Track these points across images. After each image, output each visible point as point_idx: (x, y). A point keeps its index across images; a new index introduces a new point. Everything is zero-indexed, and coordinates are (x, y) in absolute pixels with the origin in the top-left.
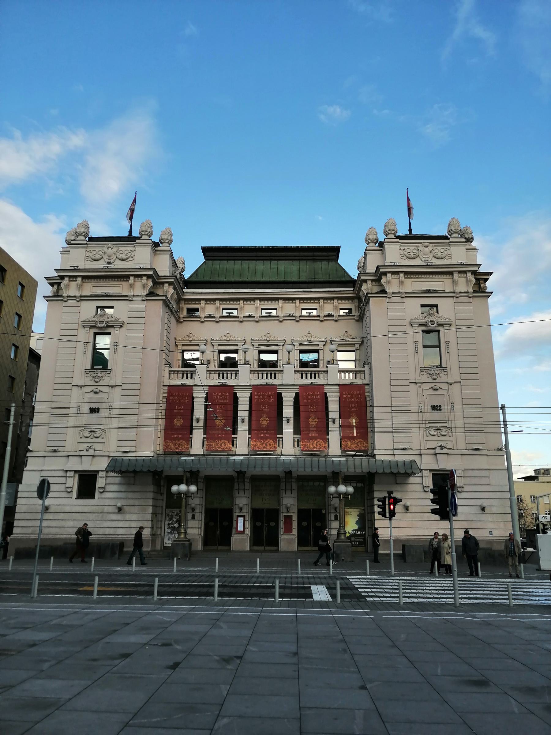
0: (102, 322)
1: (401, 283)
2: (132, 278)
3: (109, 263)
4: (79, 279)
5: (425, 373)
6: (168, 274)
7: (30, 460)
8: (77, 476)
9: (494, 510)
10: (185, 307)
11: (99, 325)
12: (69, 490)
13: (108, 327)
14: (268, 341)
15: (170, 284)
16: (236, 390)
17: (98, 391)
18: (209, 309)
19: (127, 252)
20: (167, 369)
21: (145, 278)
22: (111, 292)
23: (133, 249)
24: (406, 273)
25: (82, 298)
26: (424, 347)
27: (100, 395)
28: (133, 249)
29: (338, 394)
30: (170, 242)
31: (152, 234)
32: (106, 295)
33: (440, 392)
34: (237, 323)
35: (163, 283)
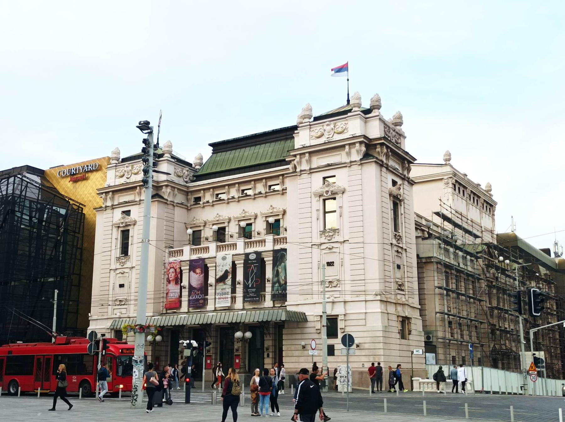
0: (122, 223)
1: (309, 161)
2: (347, 147)
3: (128, 178)
4: (111, 193)
5: (323, 236)
6: (379, 136)
7: (91, 322)
8: (113, 332)
9: (367, 346)
10: (192, 198)
11: (121, 225)
12: (318, 331)
13: (127, 226)
14: (244, 217)
15: (167, 186)
16: (207, 261)
17: (331, 247)
18: (208, 197)
19: (342, 125)
20: (167, 251)
21: (358, 145)
22: (332, 162)
23: (346, 122)
24: (310, 153)
25: (312, 171)
26: (335, 211)
27: (125, 274)
28: (346, 122)
29: (272, 258)
30: (379, 107)
31: (380, 99)
32: (126, 202)
33: (334, 250)
34: (225, 205)
35: (162, 186)
